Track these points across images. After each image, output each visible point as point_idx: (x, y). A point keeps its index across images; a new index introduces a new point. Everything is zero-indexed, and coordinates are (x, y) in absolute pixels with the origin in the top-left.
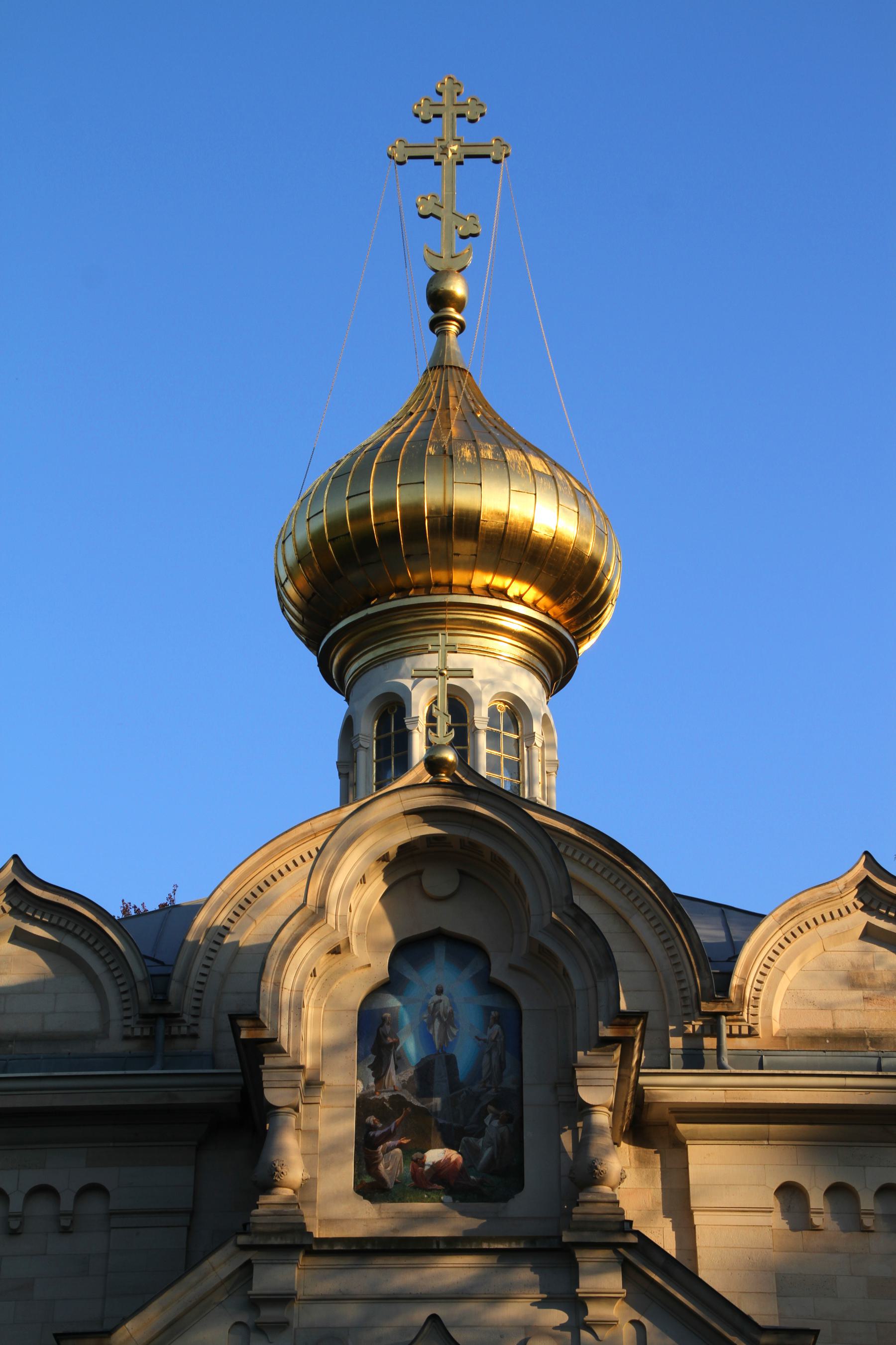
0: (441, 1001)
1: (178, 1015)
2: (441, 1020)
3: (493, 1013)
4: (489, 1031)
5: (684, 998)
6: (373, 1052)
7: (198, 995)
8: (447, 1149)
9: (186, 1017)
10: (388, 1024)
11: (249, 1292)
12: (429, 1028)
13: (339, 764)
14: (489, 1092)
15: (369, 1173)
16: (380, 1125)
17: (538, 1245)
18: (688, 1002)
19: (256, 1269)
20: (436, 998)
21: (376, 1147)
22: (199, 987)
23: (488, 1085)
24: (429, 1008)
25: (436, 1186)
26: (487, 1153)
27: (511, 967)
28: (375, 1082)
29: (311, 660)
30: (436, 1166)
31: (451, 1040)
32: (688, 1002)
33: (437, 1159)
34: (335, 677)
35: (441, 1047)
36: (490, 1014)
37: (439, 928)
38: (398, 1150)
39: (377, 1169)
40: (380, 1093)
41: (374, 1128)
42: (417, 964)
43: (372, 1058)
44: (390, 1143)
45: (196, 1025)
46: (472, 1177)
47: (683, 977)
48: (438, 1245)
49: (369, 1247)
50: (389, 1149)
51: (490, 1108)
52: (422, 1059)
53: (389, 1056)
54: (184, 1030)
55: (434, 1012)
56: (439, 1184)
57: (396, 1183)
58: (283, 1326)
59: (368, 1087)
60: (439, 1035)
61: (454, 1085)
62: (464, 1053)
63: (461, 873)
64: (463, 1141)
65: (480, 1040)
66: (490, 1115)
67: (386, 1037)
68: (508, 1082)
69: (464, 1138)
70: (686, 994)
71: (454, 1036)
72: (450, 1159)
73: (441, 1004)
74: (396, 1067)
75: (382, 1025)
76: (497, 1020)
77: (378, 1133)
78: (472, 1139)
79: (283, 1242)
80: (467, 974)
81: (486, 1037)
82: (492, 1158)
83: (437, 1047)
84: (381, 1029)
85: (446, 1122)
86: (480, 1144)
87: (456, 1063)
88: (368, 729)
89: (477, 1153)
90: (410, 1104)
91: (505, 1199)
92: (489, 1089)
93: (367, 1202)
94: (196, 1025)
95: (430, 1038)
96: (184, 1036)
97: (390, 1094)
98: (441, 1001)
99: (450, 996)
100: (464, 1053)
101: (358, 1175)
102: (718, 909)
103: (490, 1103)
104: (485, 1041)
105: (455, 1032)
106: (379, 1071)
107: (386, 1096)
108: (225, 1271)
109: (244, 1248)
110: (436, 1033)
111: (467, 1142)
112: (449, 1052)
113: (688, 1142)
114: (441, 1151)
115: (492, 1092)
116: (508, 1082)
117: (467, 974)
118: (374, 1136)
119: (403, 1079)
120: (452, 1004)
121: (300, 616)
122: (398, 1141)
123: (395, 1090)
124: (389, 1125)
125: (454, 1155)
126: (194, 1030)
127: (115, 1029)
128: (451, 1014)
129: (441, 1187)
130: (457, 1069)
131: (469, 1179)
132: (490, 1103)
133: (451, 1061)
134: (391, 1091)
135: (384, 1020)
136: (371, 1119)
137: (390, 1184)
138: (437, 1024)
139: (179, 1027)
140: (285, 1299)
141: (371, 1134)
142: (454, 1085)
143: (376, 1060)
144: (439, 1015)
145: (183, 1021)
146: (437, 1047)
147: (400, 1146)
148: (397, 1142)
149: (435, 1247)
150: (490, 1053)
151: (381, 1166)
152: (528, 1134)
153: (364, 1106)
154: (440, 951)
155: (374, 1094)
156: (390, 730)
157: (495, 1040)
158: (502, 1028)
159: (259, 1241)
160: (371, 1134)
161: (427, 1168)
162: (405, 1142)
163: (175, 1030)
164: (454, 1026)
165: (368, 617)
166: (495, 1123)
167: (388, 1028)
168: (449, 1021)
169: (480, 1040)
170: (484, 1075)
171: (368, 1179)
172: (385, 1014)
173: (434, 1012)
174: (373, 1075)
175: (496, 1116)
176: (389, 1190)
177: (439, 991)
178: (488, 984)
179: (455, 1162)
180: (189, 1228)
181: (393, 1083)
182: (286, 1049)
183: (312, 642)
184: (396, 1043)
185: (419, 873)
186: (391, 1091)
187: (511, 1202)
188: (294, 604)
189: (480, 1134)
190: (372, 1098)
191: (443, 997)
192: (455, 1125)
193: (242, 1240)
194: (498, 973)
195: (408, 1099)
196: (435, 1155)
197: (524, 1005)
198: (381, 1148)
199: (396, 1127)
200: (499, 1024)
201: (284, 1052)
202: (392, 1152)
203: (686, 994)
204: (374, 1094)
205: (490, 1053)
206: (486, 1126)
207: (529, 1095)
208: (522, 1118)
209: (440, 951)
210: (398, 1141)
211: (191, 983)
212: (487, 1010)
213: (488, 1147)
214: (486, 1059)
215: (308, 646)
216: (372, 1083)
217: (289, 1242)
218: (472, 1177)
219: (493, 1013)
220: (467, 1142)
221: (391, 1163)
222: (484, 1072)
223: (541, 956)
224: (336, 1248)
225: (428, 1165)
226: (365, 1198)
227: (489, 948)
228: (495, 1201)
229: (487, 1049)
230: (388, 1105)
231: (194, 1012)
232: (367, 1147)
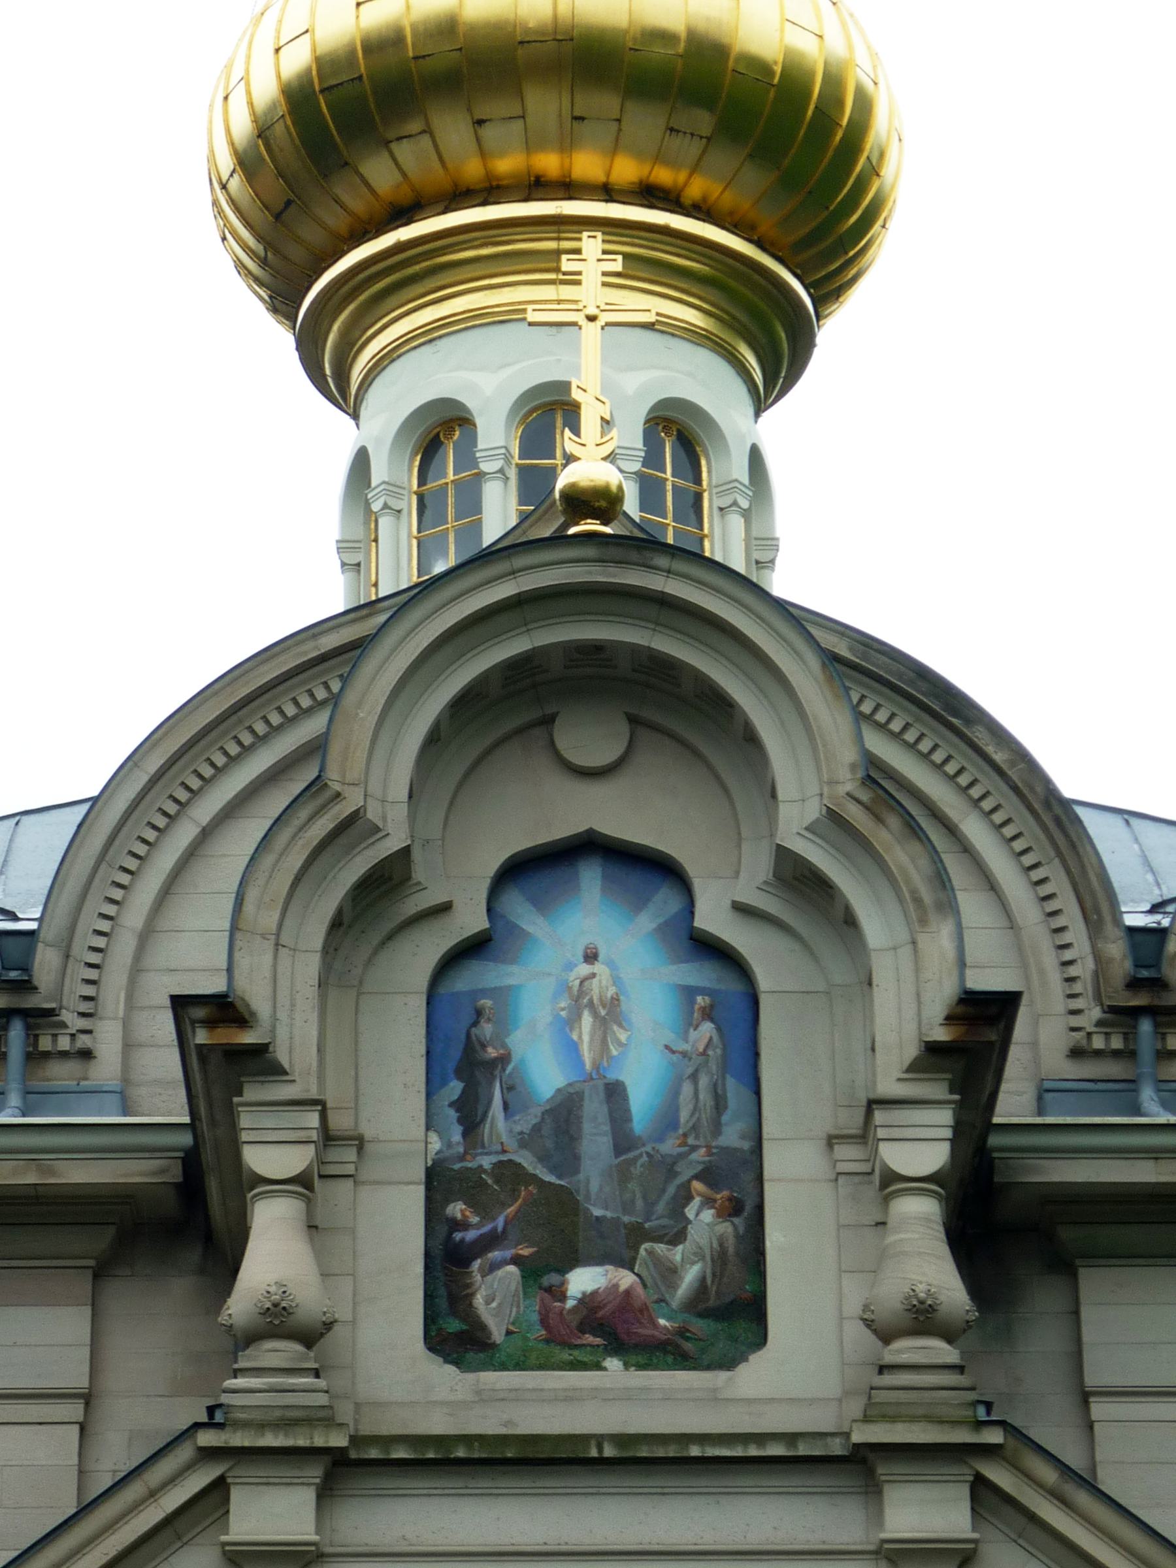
0: (594, 975)
1: (51, 1012)
2: (595, 1014)
3: (699, 999)
4: (693, 1035)
5: (1070, 980)
6: (459, 1074)
7: (92, 974)
8: (611, 1267)
9: (67, 1016)
10: (489, 1020)
11: (224, 1538)
12: (571, 1030)
13: (343, 546)
14: (694, 1156)
15: (454, 1312)
16: (475, 1220)
17: (803, 1450)
18: (1078, 988)
19: (236, 1494)
20: (584, 969)
21: (466, 1262)
22: (94, 958)
23: (691, 1141)
24: (570, 988)
25: (589, 1339)
26: (690, 1276)
27: (742, 909)
28: (465, 1135)
29: (281, 341)
30: (589, 1301)
31: (615, 1053)
32: (1078, 988)
33: (590, 1287)
34: (334, 376)
35: (597, 1067)
36: (692, 1002)
37: (590, 832)
38: (512, 1268)
39: (471, 1305)
40: (474, 1156)
41: (464, 1225)
42: (542, 904)
43: (455, 1088)
44: (495, 1255)
45: (89, 1032)
46: (662, 1322)
47: (1067, 938)
48: (600, 1448)
49: (461, 1453)
50: (494, 1267)
51: (697, 1185)
52: (559, 1090)
53: (491, 1084)
54: (64, 1043)
55: (579, 999)
56: (595, 1336)
57: (509, 1333)
59: (449, 1145)
60: (592, 1040)
61: (623, 1141)
62: (644, 1077)
63: (633, 720)
64: (642, 1252)
65: (673, 1052)
66: (697, 1200)
67: (484, 1046)
69: (646, 1245)
70: (1073, 971)
71: (620, 1044)
72: (616, 1286)
73: (595, 981)
74: (506, 1106)
75: (475, 1024)
76: (708, 1014)
77: (471, 1235)
78: (660, 1248)
79: (289, 1442)
80: (646, 922)
81: (686, 1047)
82: (702, 1288)
83: (588, 1066)
84: (473, 1029)
85: (609, 1214)
86: (678, 1258)
87: (625, 1098)
89: (670, 1274)
90: (535, 1179)
91: (729, 1364)
92: (694, 1148)
93: (451, 1369)
94: (89, 1032)
95: (573, 1048)
96: (64, 1055)
97: (494, 1159)
98: (594, 975)
99: (611, 964)
100: (644, 1077)
101: (430, 1319)
102: (1117, 821)
103: (696, 1177)
104: (684, 1054)
105: (623, 1036)
106: (470, 1115)
107: (486, 1162)
109: (210, 1454)
110: (586, 1038)
111: (650, 1253)
112: (612, 1076)
113: (1078, 1262)
114: (598, 1270)
115: (700, 1155)
116: (732, 1136)
117: (646, 922)
118: (462, 1240)
119: (518, 1128)
120: (616, 980)
121: (259, 248)
122: (513, 1251)
123: (504, 1151)
124: (494, 1219)
125: (626, 1279)
126: (84, 1041)
128: (615, 1000)
129: (598, 1341)
130: (627, 1111)
131: (655, 1325)
132: (696, 1177)
133: (615, 1093)
134: (496, 1153)
135: (479, 1013)
136: (457, 1209)
137: (498, 1336)
138: (587, 1020)
139: (55, 1036)
141: (458, 1236)
142: (623, 1141)
143: (463, 1092)
144: (591, 1005)
145: (63, 1025)
146: (588, 1066)
147: (516, 1260)
148: (508, 1254)
149: (594, 1453)
150: (694, 1077)
151: (479, 1300)
152: (774, 1238)
153: (440, 1182)
154: (590, 876)
155: (462, 1158)
156: (445, 476)
157: (704, 1053)
158: (719, 1029)
159: (239, 1439)
160: (458, 1236)
161: (570, 1303)
162: (526, 1252)
163: (45, 1044)
164: (620, 1026)
165: (400, 247)
166: (708, 1215)
167: (486, 1029)
168: (611, 1014)
169: (673, 1052)
170: (682, 1120)
171: (453, 1325)
172: (482, 1002)
173: (579, 999)
174: (460, 1121)
175: (708, 1202)
176: (494, 1346)
177: (591, 957)
179: (628, 1293)
180: (83, 1428)
181: (499, 1136)
182: (286, 1066)
183: (282, 302)
184: (505, 1059)
185: (548, 721)
186: (496, 1153)
187: (743, 1369)
188: (248, 225)
189: (678, 1238)
190: (457, 1166)
191: (598, 968)
192: (626, 1219)
193: (206, 1438)
194: (712, 918)
195: (530, 1169)
196: (583, 1281)
197: (764, 982)
198: (477, 1264)
199: (506, 1223)
200: (712, 1020)
201: (286, 1073)
202: (500, 1273)
203: (1073, 971)
204: (462, 1158)
205: (694, 1077)
206: (689, 1222)
207: (774, 1161)
208: (760, 1209)
210: (513, 1251)
211: (79, 950)
212: (689, 993)
213: (693, 1263)
214: (687, 1089)
215: (274, 310)
216: (456, 1135)
217: (301, 1442)
218: (662, 1322)
219: (699, 999)
220: (650, 1253)
221: (496, 1294)
222: (684, 1115)
223: (799, 880)
224: (394, 1456)
225: (574, 1298)
226: (446, 1361)
228: (708, 1368)
229: (690, 1070)
230: (490, 1181)
231: (85, 1007)
232: (448, 1264)
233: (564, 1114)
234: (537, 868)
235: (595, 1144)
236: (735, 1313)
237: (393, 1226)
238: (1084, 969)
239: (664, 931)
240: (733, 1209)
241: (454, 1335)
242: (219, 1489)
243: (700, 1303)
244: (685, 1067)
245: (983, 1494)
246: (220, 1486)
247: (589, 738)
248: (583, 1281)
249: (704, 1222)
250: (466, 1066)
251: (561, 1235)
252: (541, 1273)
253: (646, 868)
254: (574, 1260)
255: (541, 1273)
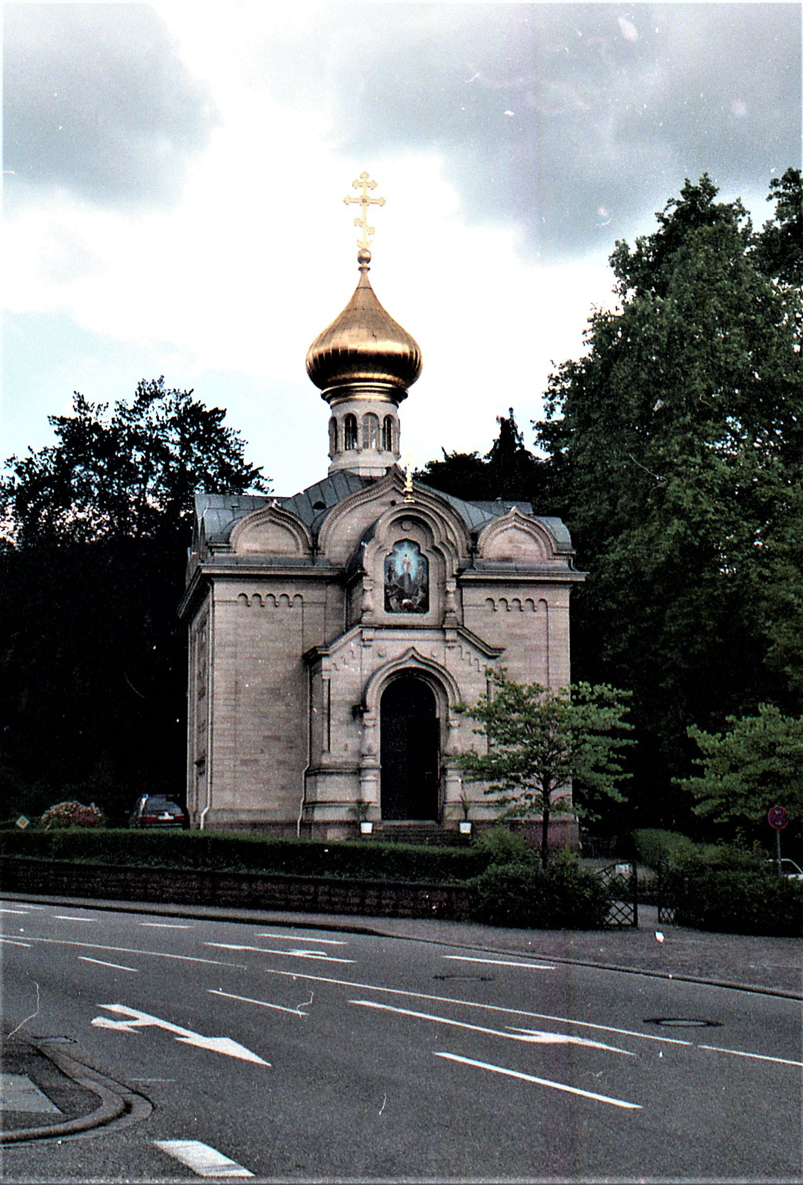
58: (370, 646)
61: (410, 583)
62: (413, 573)
68: (424, 582)
88: (342, 424)
89: (416, 600)
100: (413, 573)
106: (390, 578)
108: (356, 632)
127: (301, 551)
133: (409, 575)
140: (371, 640)
153: (386, 587)
178: (419, 554)
196: (405, 601)
209: (406, 544)
212: (419, 562)
221: (393, 602)
227: (419, 542)
233: (402, 578)
234: (399, 543)
235: (407, 583)
236: (424, 607)
237: (380, 593)
238: (465, 545)
239: (415, 553)
240: (424, 592)
241: (388, 608)
242: (361, 632)
243: (420, 604)
244: (419, 573)
245: (459, 634)
246: (361, 632)
247: (406, 525)
248: (405, 601)
249: (421, 593)
250: (389, 570)
251: (401, 595)
252: (399, 600)
253: (413, 543)
254: (403, 598)
255: (399, 600)
